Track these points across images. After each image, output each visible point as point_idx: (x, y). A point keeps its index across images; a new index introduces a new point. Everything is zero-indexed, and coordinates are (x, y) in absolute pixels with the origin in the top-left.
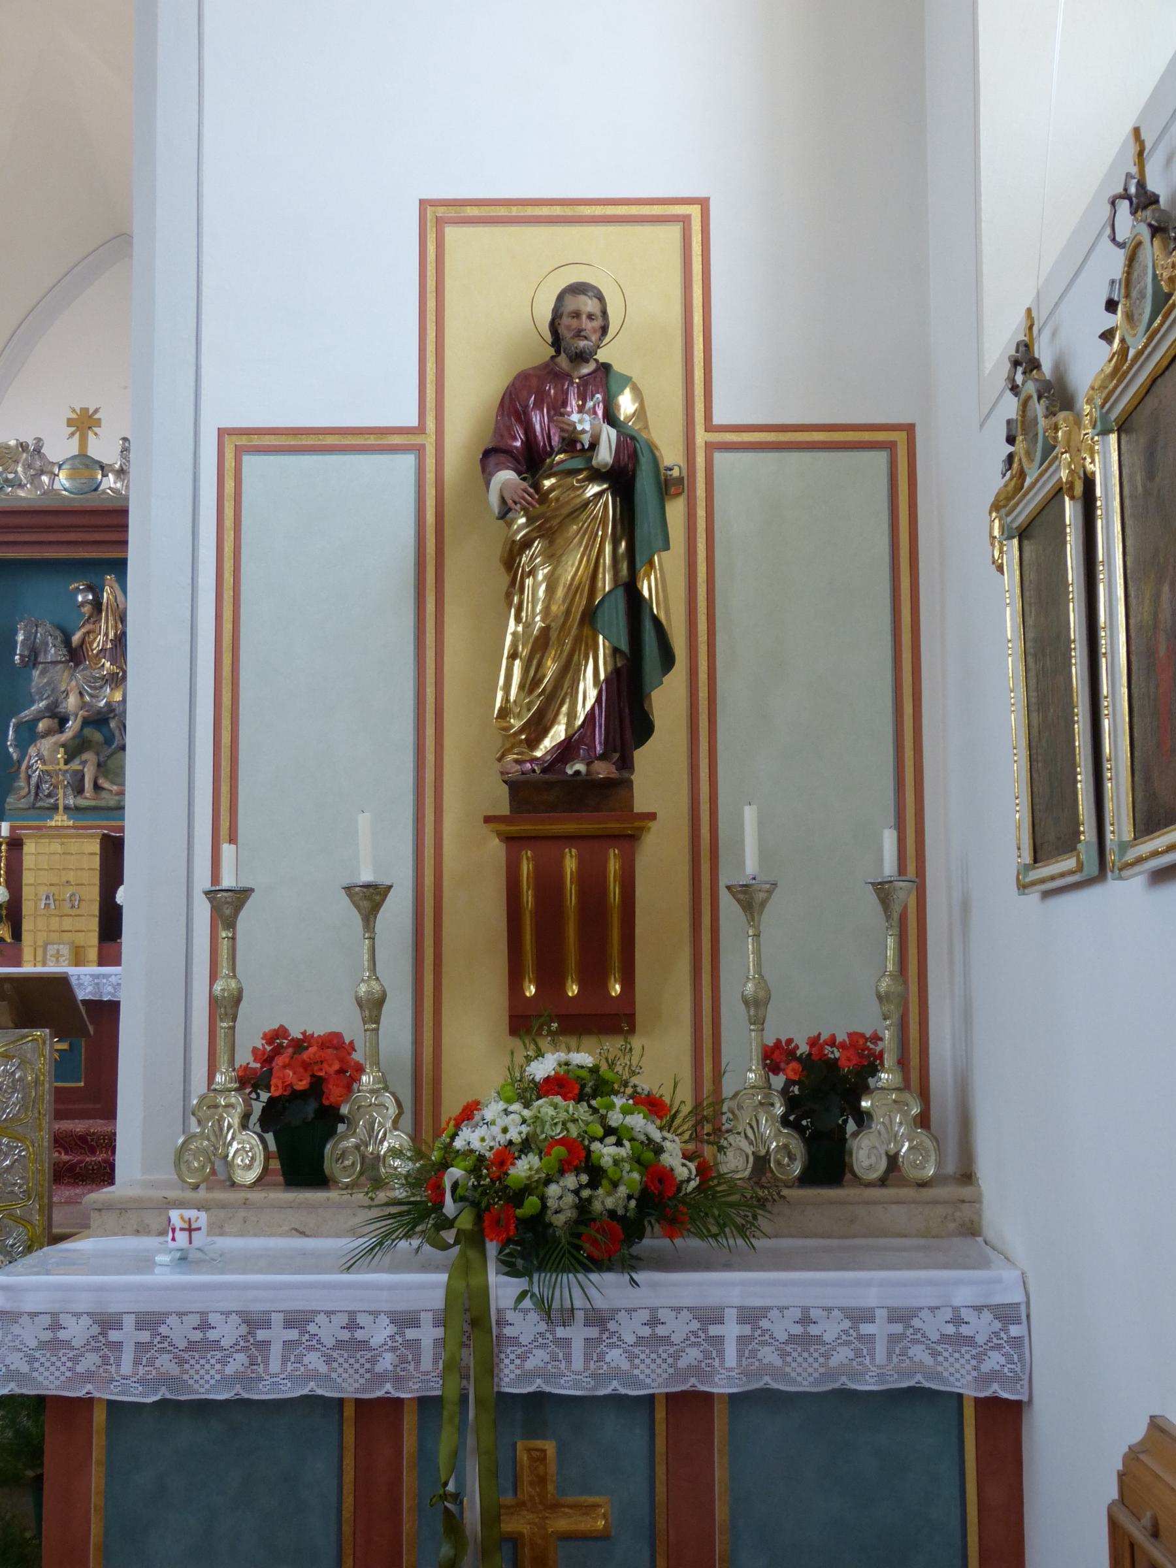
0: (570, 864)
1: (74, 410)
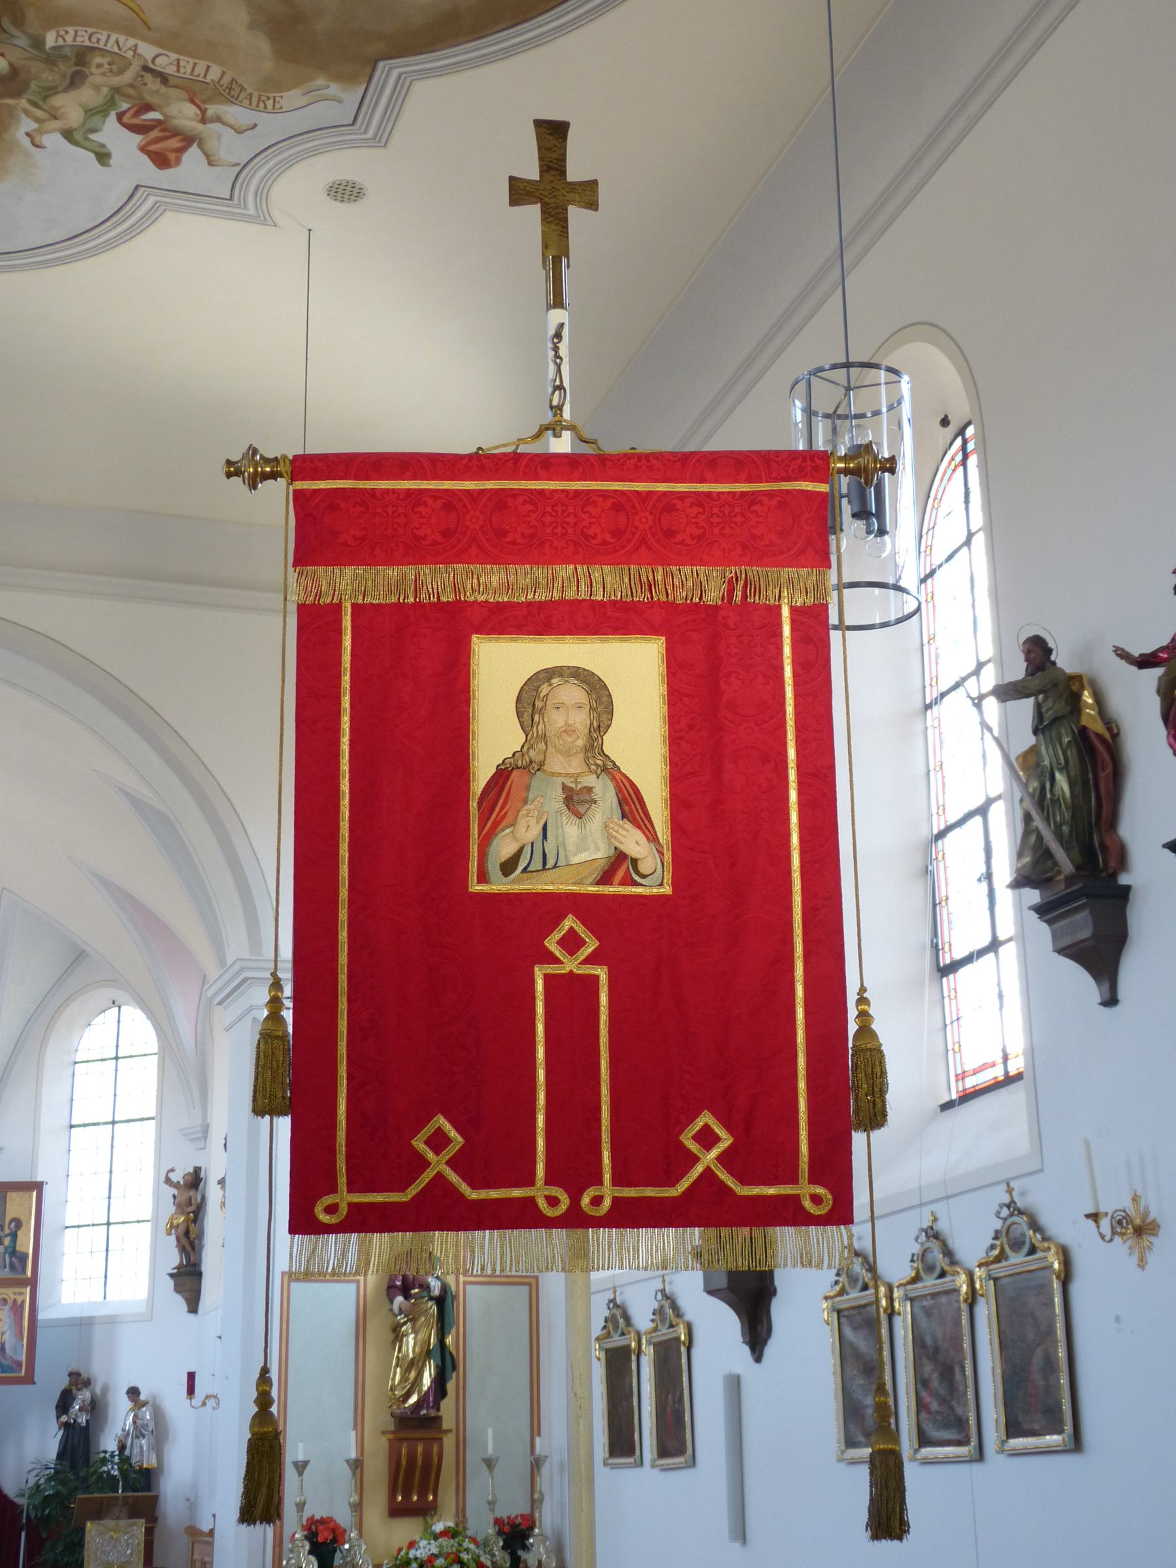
0: (420, 1449)
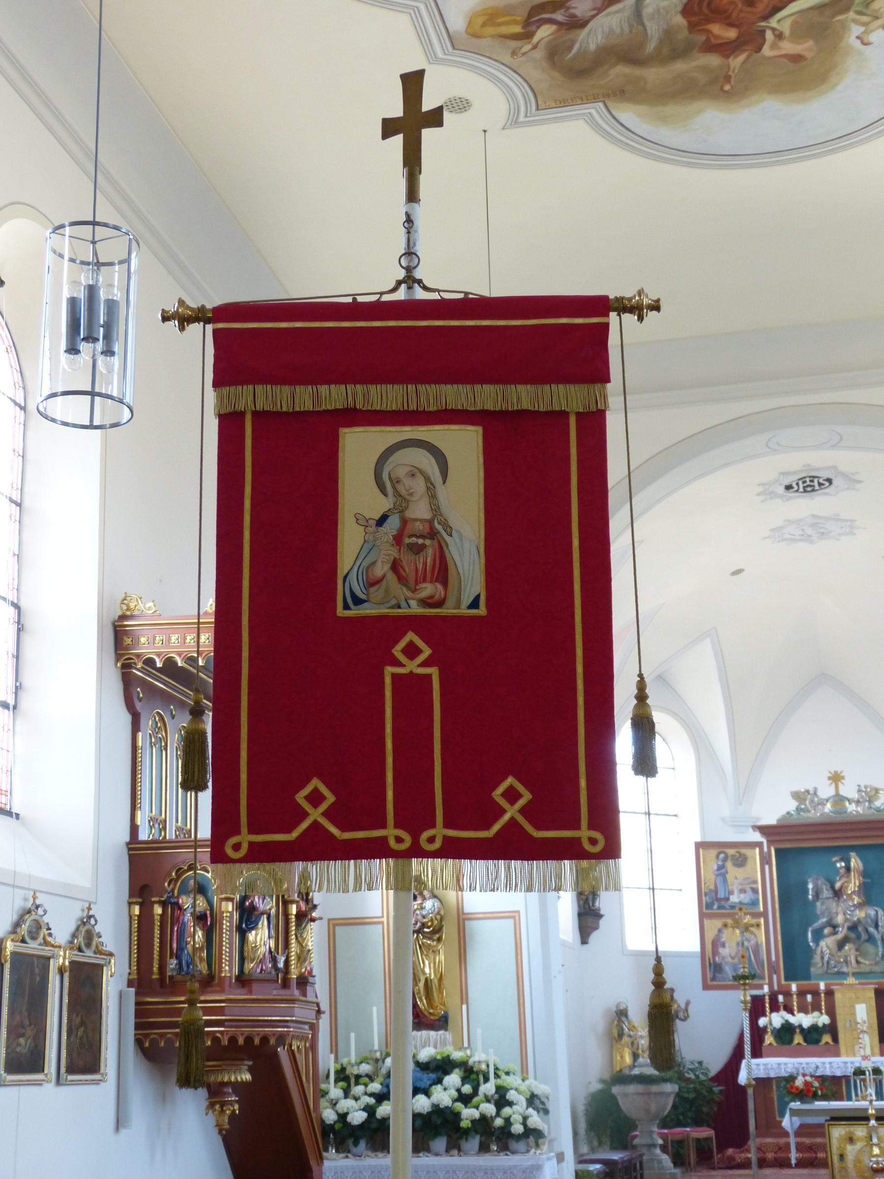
1: (830, 772)
